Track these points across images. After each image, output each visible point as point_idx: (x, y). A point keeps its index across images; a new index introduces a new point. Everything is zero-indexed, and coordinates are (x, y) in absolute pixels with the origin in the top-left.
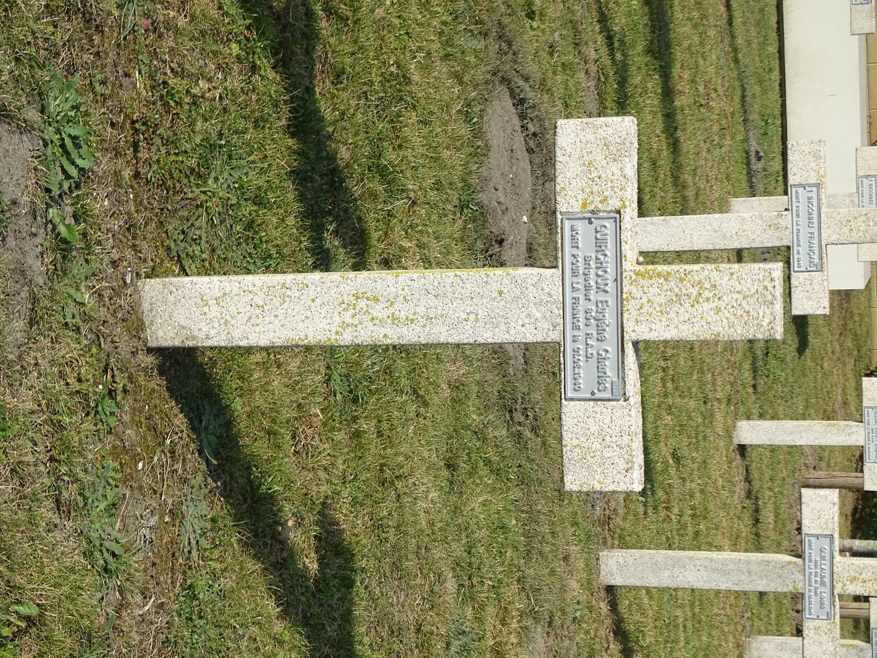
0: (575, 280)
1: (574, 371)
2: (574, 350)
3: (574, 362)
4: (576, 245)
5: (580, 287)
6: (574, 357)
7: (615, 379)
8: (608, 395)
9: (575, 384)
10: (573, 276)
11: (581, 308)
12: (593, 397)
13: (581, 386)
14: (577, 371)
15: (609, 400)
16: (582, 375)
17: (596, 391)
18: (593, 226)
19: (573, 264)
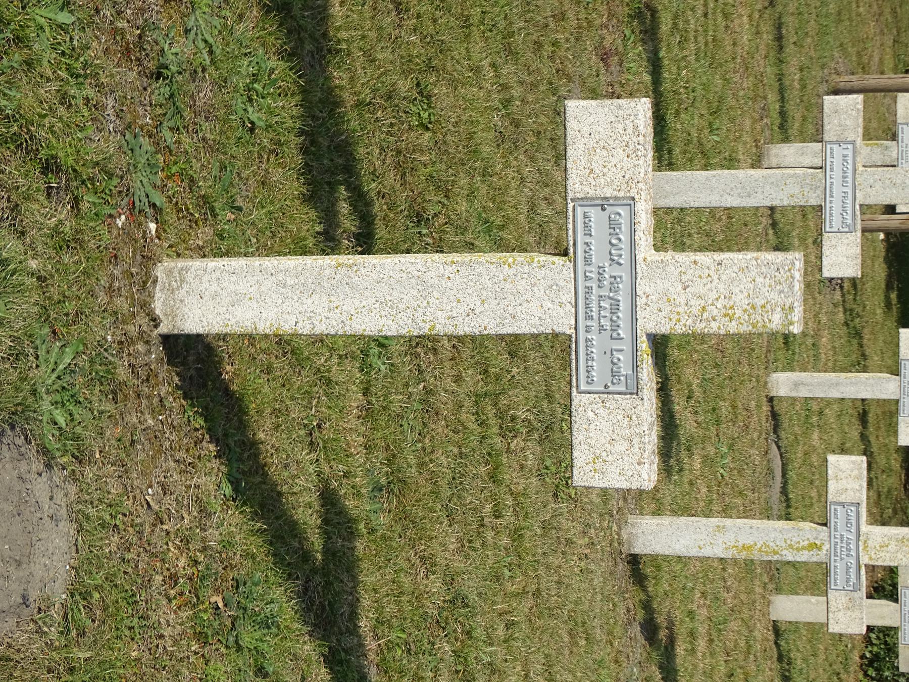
0: (588, 268)
1: (587, 363)
2: (586, 341)
3: (587, 354)
4: (589, 232)
5: (593, 276)
6: (587, 350)
7: (631, 372)
8: (623, 389)
9: (588, 377)
11: (594, 298)
12: (607, 391)
13: (595, 379)
14: (590, 364)
16: (595, 368)
17: (609, 385)
18: (607, 213)
19: (585, 252)
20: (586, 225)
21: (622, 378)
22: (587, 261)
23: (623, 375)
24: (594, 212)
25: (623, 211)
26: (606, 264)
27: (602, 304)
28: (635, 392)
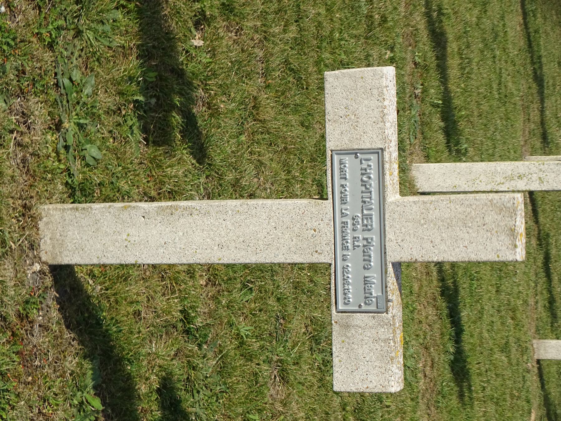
0: (344, 206)
1: (344, 287)
2: (343, 268)
3: (344, 279)
4: (344, 176)
5: (348, 213)
6: (344, 275)
7: (380, 294)
8: (373, 308)
9: (345, 298)
11: (349, 231)
13: (351, 300)
14: (346, 287)
16: (351, 291)
18: (359, 160)
19: (341, 193)
20: (342, 171)
21: (374, 300)
22: (343, 201)
23: (374, 297)
24: (347, 159)
25: (373, 157)
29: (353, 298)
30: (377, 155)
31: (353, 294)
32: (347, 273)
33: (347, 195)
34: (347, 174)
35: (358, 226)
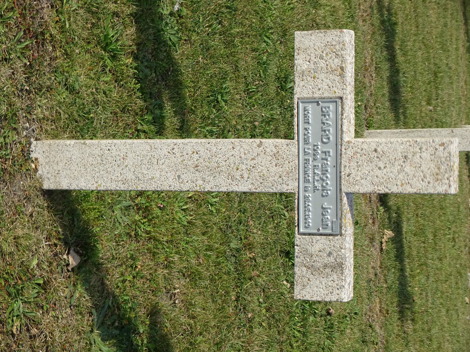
0: (306, 146)
2: (305, 198)
3: (305, 207)
4: (307, 121)
5: (310, 152)
7: (335, 220)
8: (329, 232)
9: (306, 223)
10: (305, 144)
11: (310, 167)
12: (318, 233)
13: (310, 224)
14: (307, 214)
15: (330, 235)
16: (311, 216)
17: (320, 229)
19: (305, 135)
20: (305, 116)
22: (306, 142)
24: (310, 107)
25: (332, 106)
26: (319, 143)
27: (316, 171)
28: (338, 233)
29: (312, 215)
30: (335, 103)
31: (312, 219)
32: (308, 202)
33: (309, 137)
34: (310, 119)
35: (318, 156)
